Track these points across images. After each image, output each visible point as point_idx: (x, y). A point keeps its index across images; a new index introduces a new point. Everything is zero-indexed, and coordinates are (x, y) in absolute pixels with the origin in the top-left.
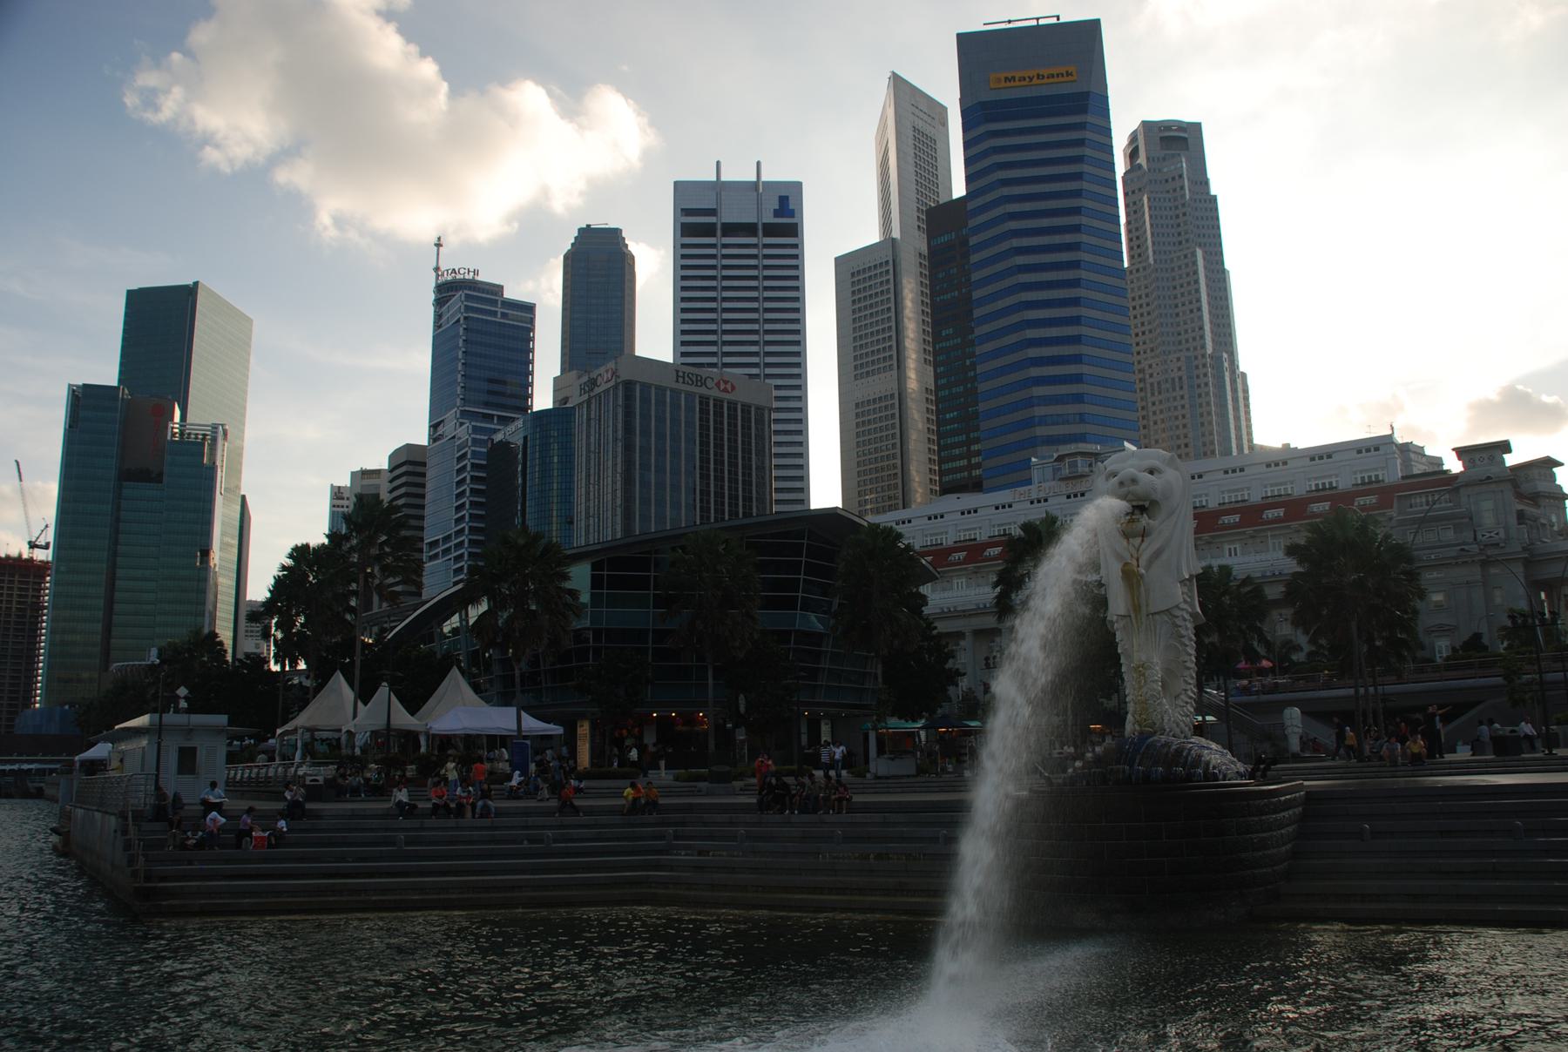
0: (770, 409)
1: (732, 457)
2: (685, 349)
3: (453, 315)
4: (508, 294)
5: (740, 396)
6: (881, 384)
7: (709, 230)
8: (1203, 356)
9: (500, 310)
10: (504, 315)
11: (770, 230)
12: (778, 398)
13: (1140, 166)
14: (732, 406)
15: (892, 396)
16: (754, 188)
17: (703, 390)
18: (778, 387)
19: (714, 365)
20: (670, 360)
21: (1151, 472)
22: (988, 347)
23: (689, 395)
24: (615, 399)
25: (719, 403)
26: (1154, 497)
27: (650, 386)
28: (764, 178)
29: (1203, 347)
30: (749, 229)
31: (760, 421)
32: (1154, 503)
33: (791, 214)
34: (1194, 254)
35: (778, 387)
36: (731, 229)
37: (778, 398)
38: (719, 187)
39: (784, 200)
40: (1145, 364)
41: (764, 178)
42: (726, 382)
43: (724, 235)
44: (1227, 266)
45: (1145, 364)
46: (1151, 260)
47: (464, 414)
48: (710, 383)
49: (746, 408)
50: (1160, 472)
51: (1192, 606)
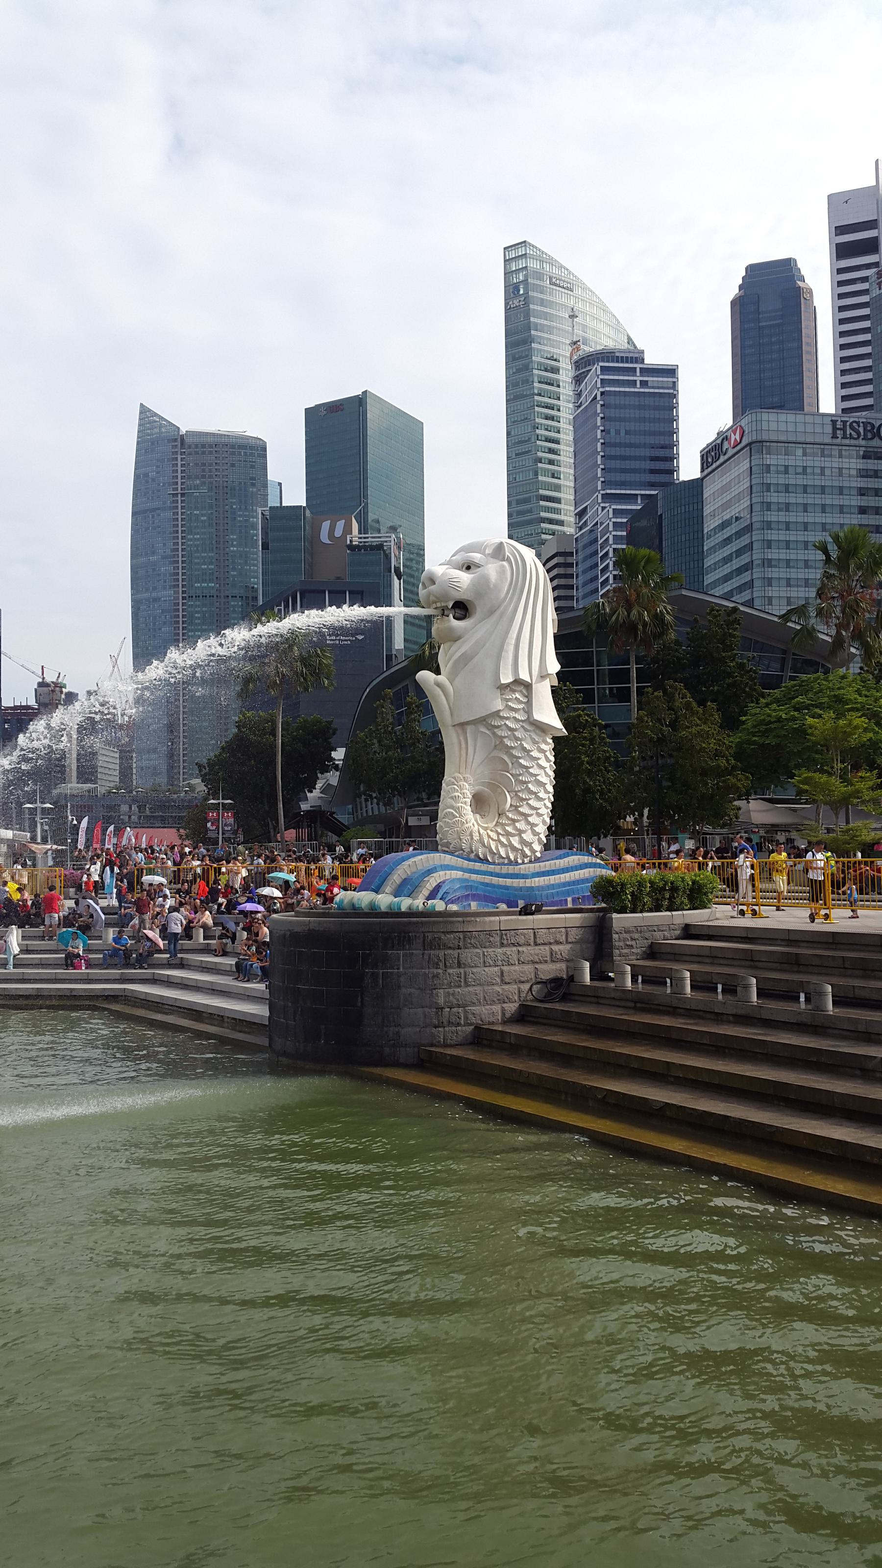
2: (845, 392)
3: (591, 392)
4: (651, 359)
9: (638, 379)
10: (644, 384)
21: (468, 568)
26: (459, 596)
47: (606, 497)
50: (478, 566)
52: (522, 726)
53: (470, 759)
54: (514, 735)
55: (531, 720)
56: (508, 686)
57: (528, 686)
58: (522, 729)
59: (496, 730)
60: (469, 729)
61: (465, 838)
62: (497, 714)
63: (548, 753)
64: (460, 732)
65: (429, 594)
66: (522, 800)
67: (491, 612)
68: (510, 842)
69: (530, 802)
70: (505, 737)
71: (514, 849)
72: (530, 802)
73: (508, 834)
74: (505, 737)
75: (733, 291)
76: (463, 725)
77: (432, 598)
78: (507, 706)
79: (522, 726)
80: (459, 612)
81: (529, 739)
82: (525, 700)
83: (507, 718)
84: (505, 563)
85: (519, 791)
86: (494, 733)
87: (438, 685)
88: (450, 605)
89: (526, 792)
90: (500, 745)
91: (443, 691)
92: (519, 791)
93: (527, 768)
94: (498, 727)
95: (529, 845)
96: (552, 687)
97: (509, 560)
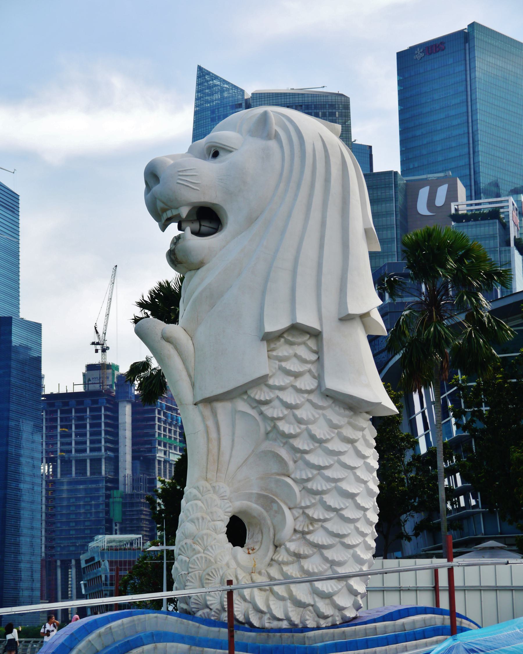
21: (216, 155)
51: (319, 378)
52: (309, 401)
53: (225, 457)
54: (295, 416)
55: (323, 389)
56: (279, 336)
57: (316, 335)
58: (308, 406)
59: (264, 408)
60: (223, 409)
62: (262, 381)
63: (360, 446)
64: (207, 412)
66: (313, 521)
67: (251, 220)
68: (290, 592)
69: (328, 525)
70: (279, 419)
71: (300, 604)
72: (328, 525)
74: (279, 419)
76: (209, 401)
79: (309, 401)
80: (206, 226)
81: (322, 422)
82: (314, 357)
83: (281, 388)
84: (273, 144)
85: (307, 507)
86: (261, 413)
88: (184, 212)
89: (319, 507)
90: (274, 432)
91: (176, 348)
92: (307, 507)
93: (320, 468)
94: (266, 403)
95: (328, 597)
96: (373, 340)
97: (277, 137)
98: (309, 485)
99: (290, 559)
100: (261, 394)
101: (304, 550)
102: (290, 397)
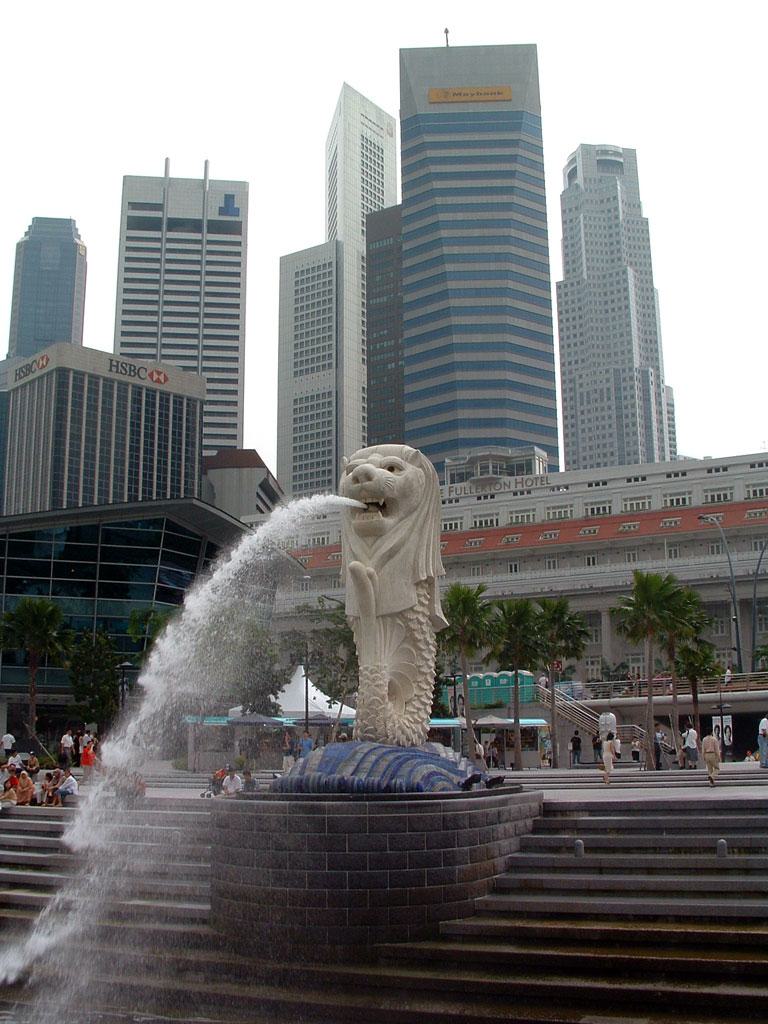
0: (203, 403)
1: (163, 447)
5: (173, 387)
6: (321, 382)
7: (154, 224)
8: (631, 369)
11: (215, 227)
12: (209, 391)
13: (577, 186)
14: (165, 396)
15: (330, 393)
16: (200, 187)
17: (136, 381)
18: (210, 380)
19: (153, 356)
20: (110, 350)
21: (391, 469)
22: (418, 349)
23: (123, 386)
24: (49, 388)
25: (151, 393)
26: (389, 494)
27: (83, 374)
28: (211, 176)
29: (631, 360)
30: (195, 225)
31: (191, 413)
32: (393, 501)
33: (236, 212)
34: (625, 272)
35: (210, 380)
36: (175, 224)
37: (209, 391)
38: (166, 183)
39: (229, 198)
40: (575, 375)
41: (211, 176)
42: (159, 373)
43: (169, 229)
44: (657, 284)
45: (575, 375)
46: (585, 276)
48: (143, 374)
49: (178, 399)
51: (431, 607)
61: (390, 725)
62: (412, 609)
65: (362, 488)
67: (410, 513)
73: (416, 722)
75: (18, 232)
76: (383, 616)
77: (364, 493)
78: (419, 601)
83: (418, 612)
86: (407, 627)
87: (371, 576)
94: (411, 620)
98: (423, 670)
99: (416, 711)
100: (411, 616)
101: (422, 707)
102: (422, 619)
